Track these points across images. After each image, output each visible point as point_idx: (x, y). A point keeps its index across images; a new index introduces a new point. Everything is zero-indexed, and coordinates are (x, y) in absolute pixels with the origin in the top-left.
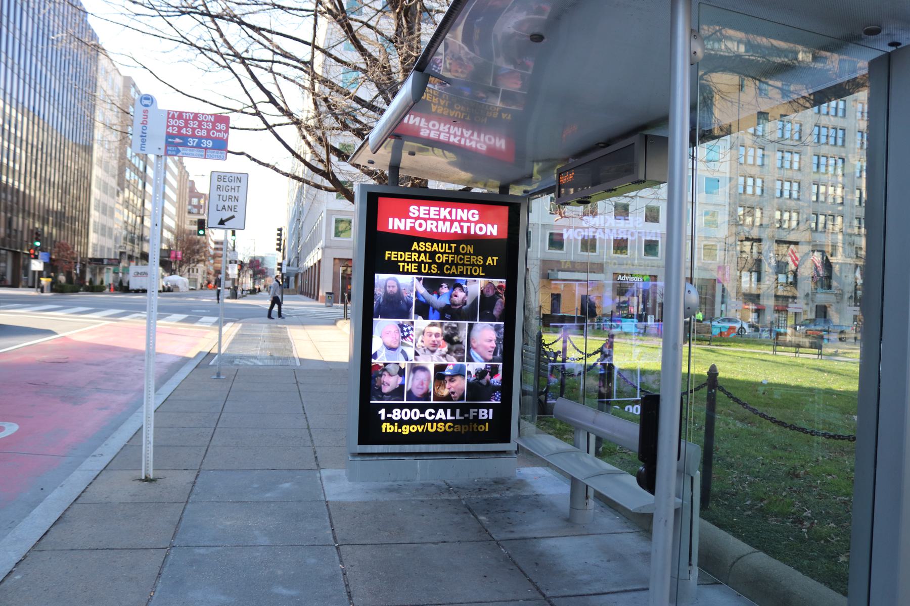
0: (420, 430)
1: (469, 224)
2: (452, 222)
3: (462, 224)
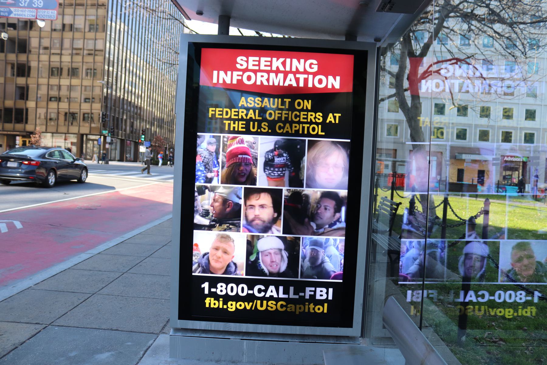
0: (248, 308)
1: (306, 76)
2: (286, 74)
3: (298, 76)
